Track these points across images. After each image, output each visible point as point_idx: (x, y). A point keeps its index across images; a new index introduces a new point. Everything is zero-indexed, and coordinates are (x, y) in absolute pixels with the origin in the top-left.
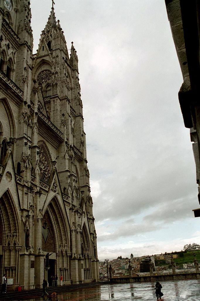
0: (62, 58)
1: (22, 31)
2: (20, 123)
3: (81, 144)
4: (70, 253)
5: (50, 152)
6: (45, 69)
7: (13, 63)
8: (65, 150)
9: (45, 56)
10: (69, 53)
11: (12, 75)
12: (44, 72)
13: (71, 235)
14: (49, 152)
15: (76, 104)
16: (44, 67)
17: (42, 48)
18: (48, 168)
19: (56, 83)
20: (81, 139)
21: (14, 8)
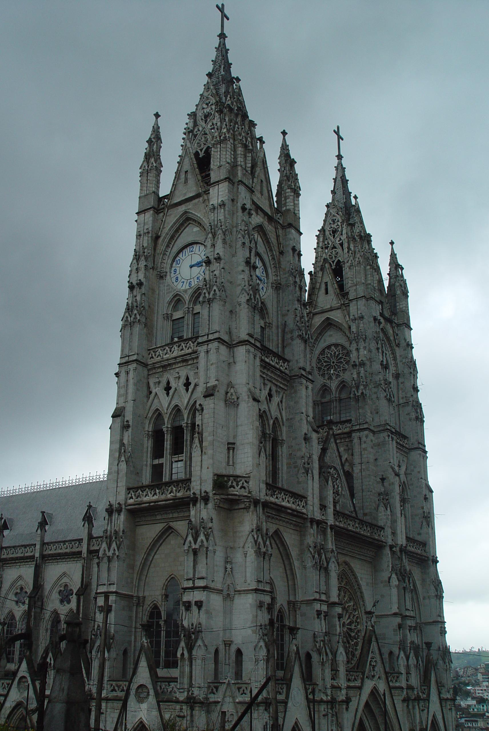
0: (372, 319)
1: (292, 339)
2: (305, 567)
3: (424, 521)
5: (358, 575)
6: (333, 341)
7: (281, 424)
8: (388, 566)
9: (331, 310)
10: (385, 269)
11: (280, 453)
12: (333, 347)
14: (356, 578)
16: (331, 336)
17: (323, 286)
18: (357, 613)
19: (362, 393)
20: (423, 508)
21: (271, 281)
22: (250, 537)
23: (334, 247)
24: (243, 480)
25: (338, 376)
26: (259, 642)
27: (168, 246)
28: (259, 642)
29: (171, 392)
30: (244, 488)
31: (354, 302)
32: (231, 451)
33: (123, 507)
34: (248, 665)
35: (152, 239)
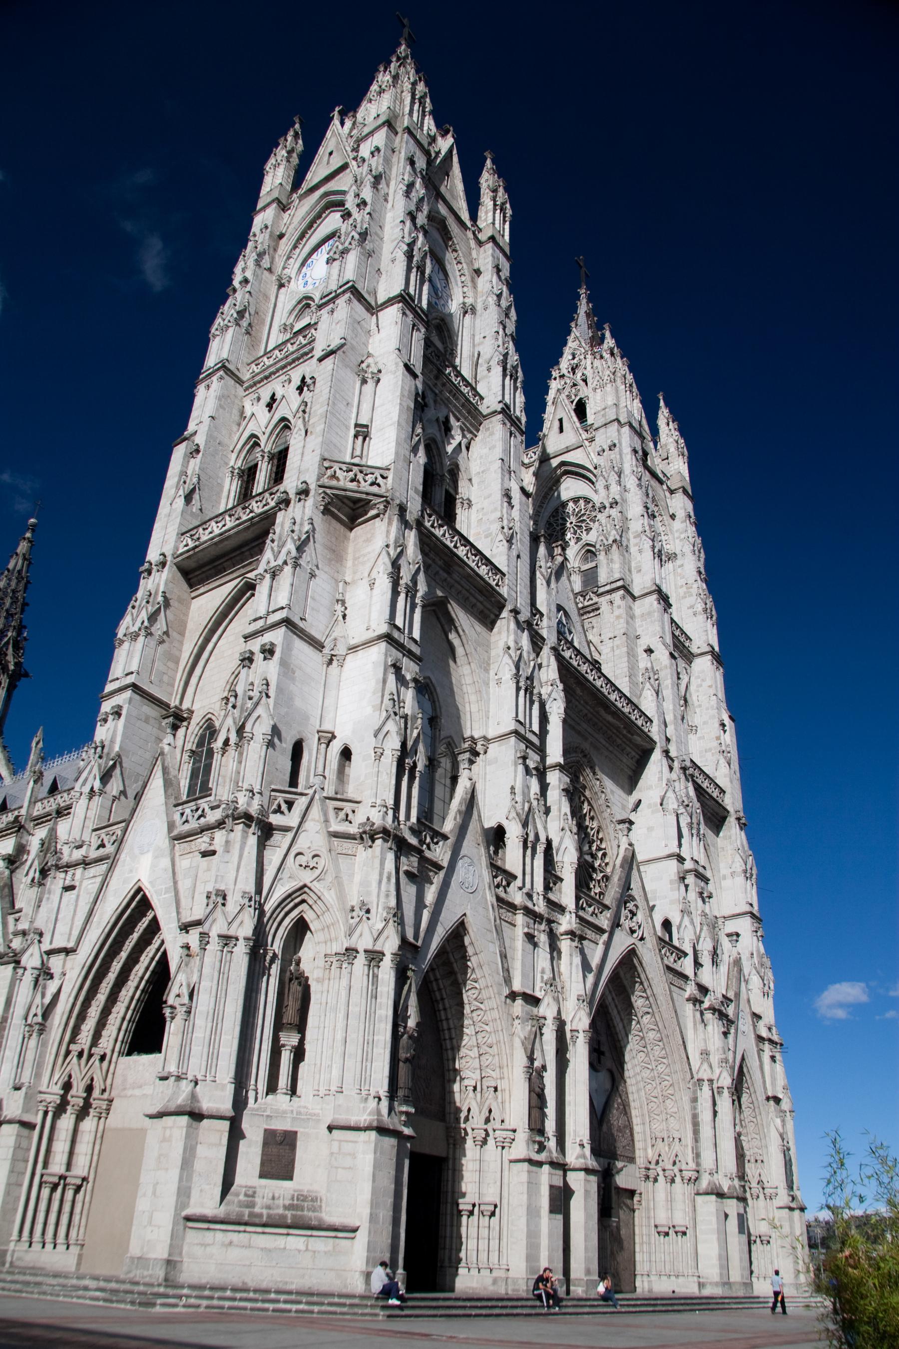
1: (489, 370)
4: (692, 1165)
13: (695, 1100)
15: (691, 611)
17: (557, 424)
22: (384, 553)
23: (575, 385)
24: (377, 473)
25: (578, 539)
26: (384, 723)
27: (295, 247)
28: (384, 723)
29: (275, 406)
30: (379, 485)
31: (602, 430)
32: (360, 438)
33: (169, 558)
34: (358, 766)
35: (271, 236)
